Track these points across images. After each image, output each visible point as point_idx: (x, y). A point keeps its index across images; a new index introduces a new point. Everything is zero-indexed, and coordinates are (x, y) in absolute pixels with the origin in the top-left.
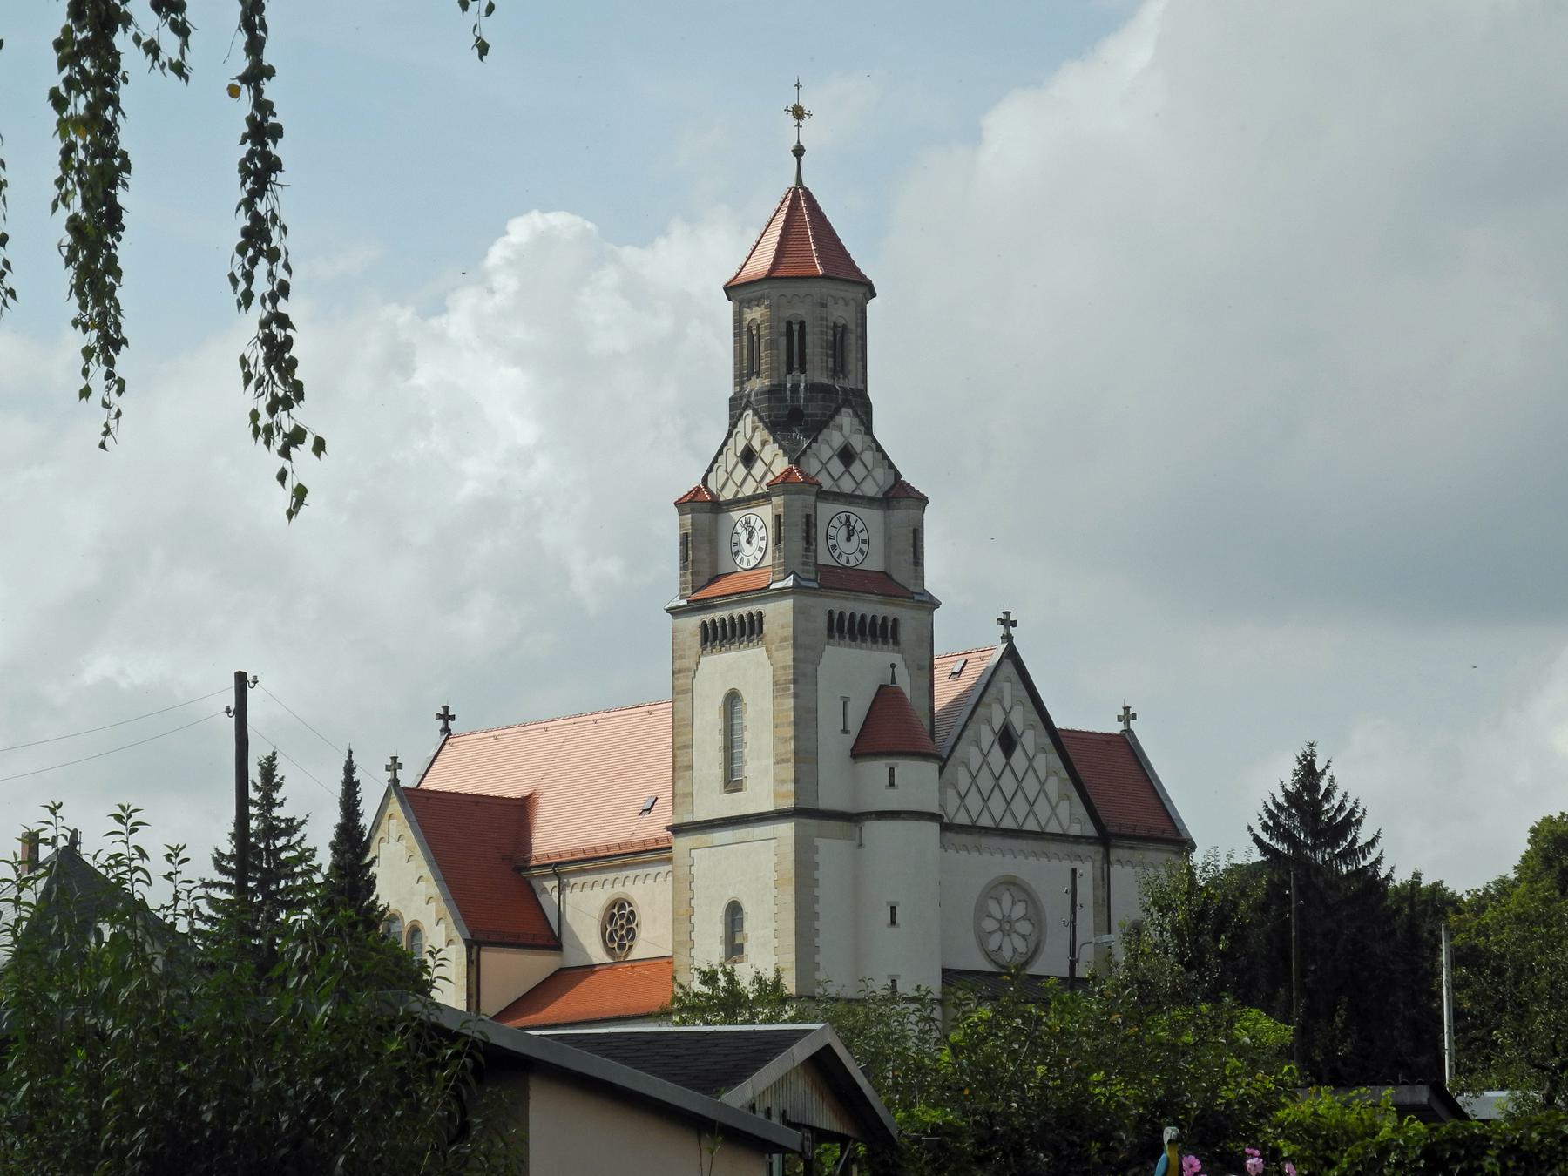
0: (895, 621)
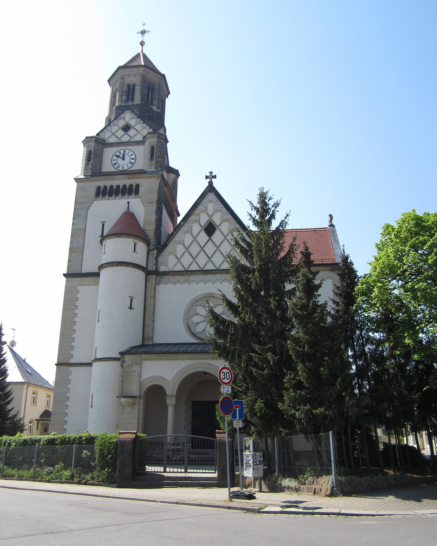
0: (138, 186)
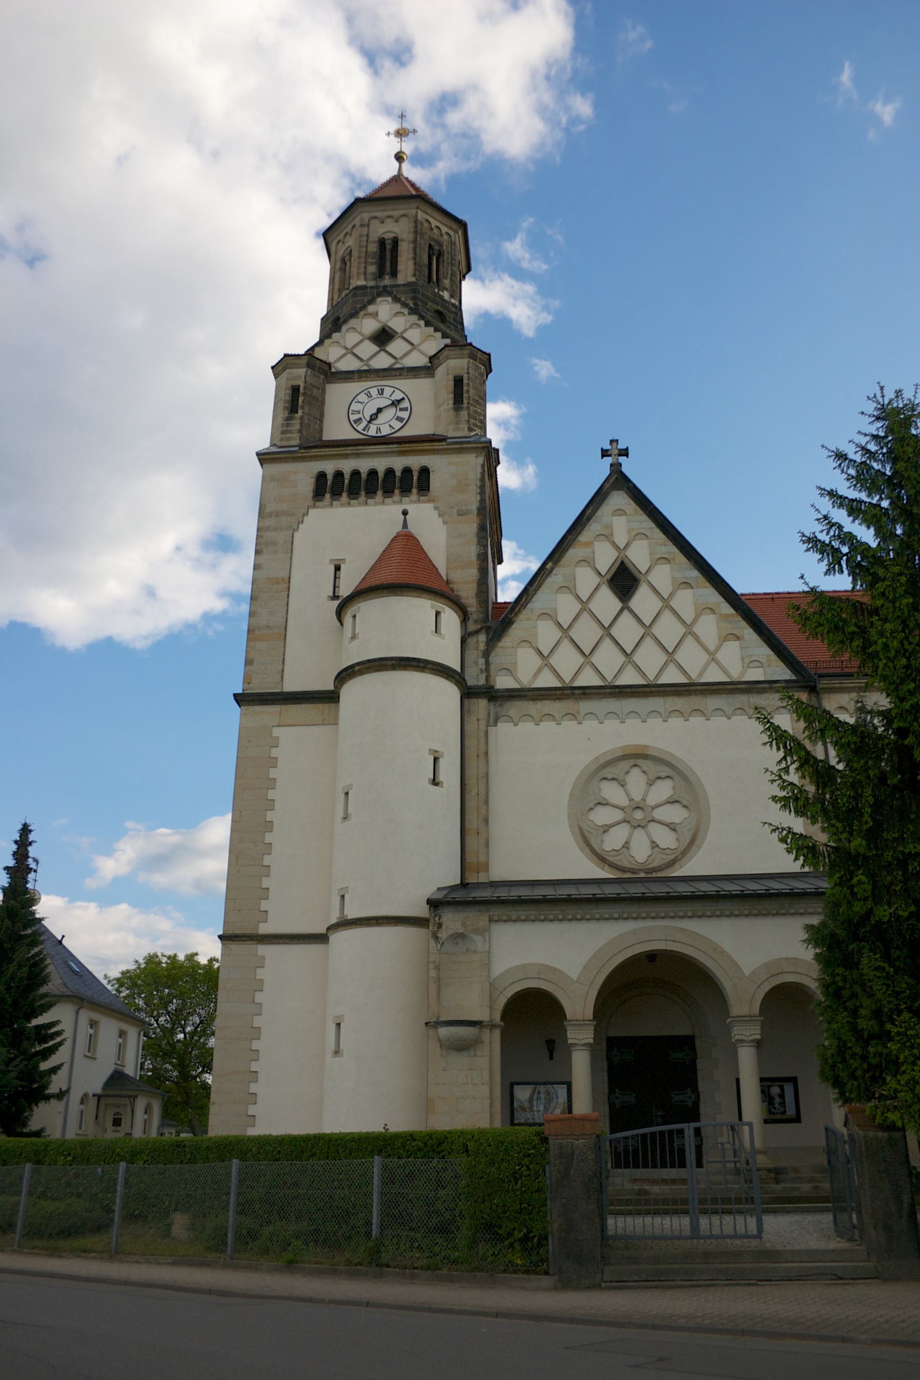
0: (425, 472)
